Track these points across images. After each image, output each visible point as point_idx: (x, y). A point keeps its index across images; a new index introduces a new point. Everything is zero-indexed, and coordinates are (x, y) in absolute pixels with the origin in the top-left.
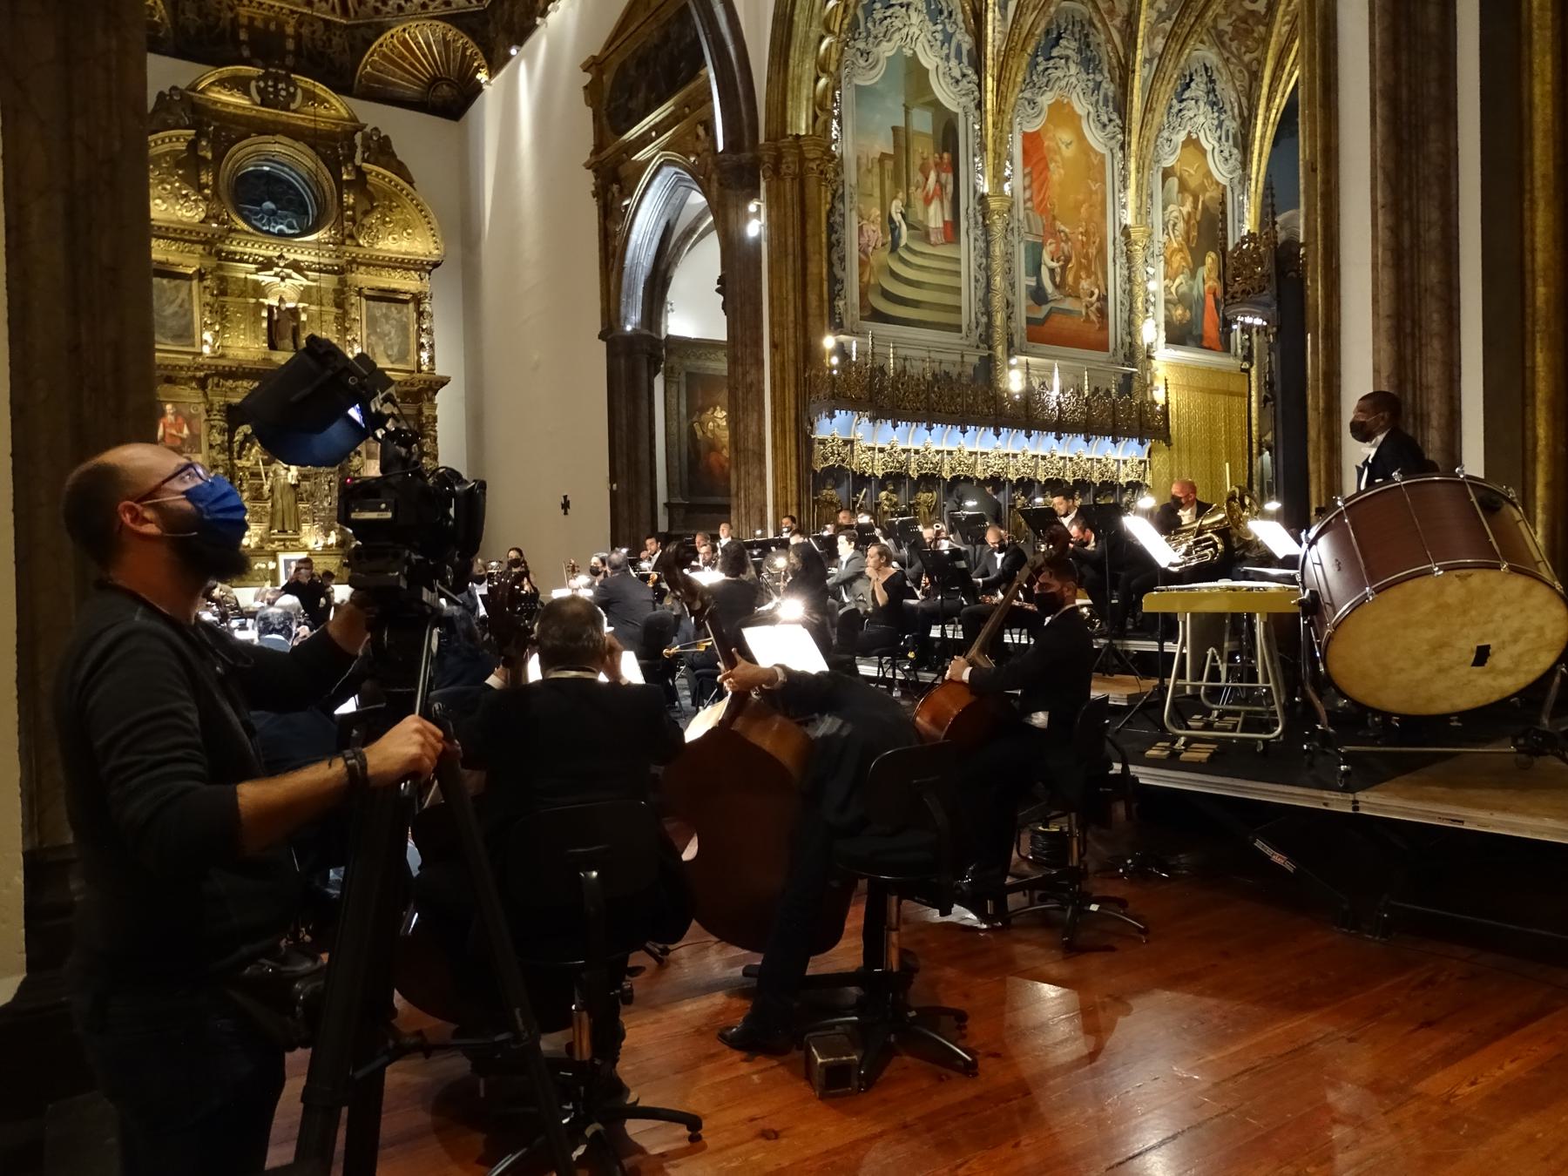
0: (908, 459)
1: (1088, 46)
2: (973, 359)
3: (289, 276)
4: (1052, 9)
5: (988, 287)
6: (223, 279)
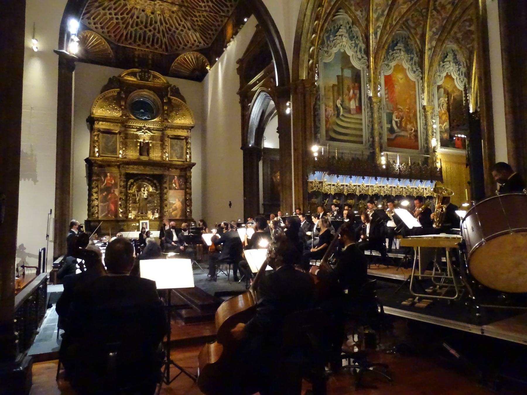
0: (343, 188)
1: (408, 45)
2: (367, 153)
3: (147, 132)
4: (394, 34)
5: (373, 129)
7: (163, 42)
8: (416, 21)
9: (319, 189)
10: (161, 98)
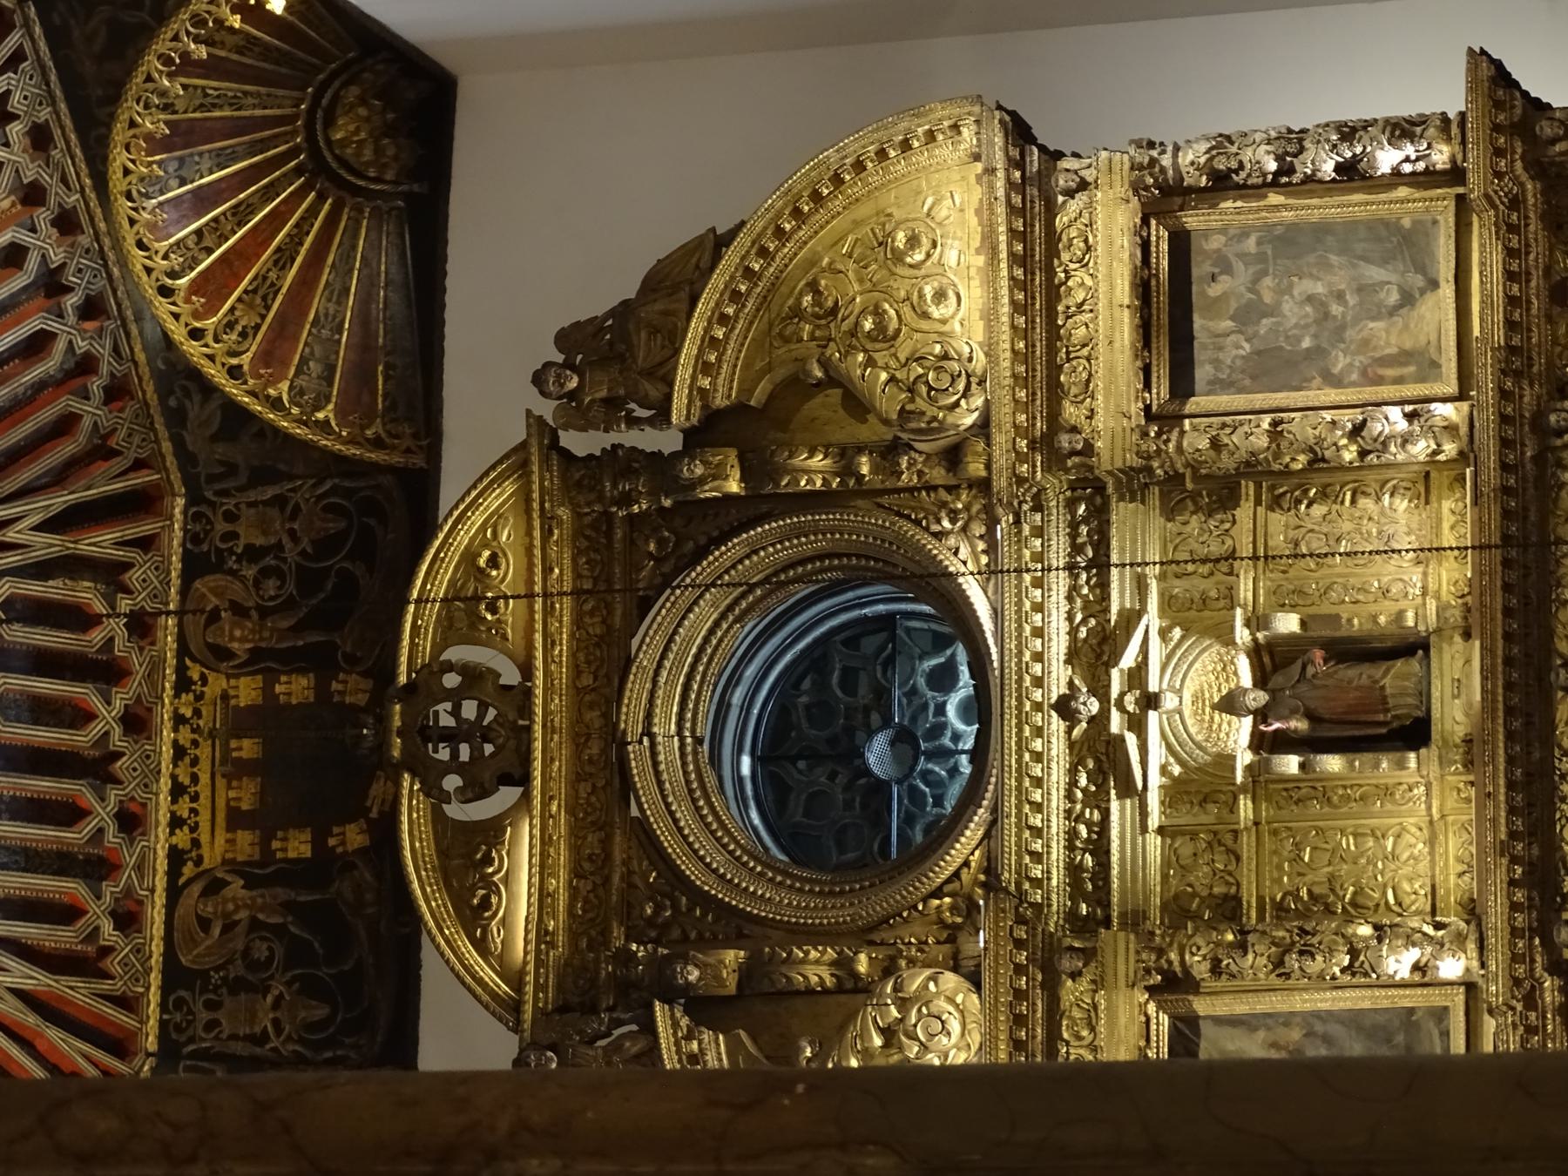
3: (1137, 676)
6: (1179, 912)
7: (49, 545)
10: (703, 526)
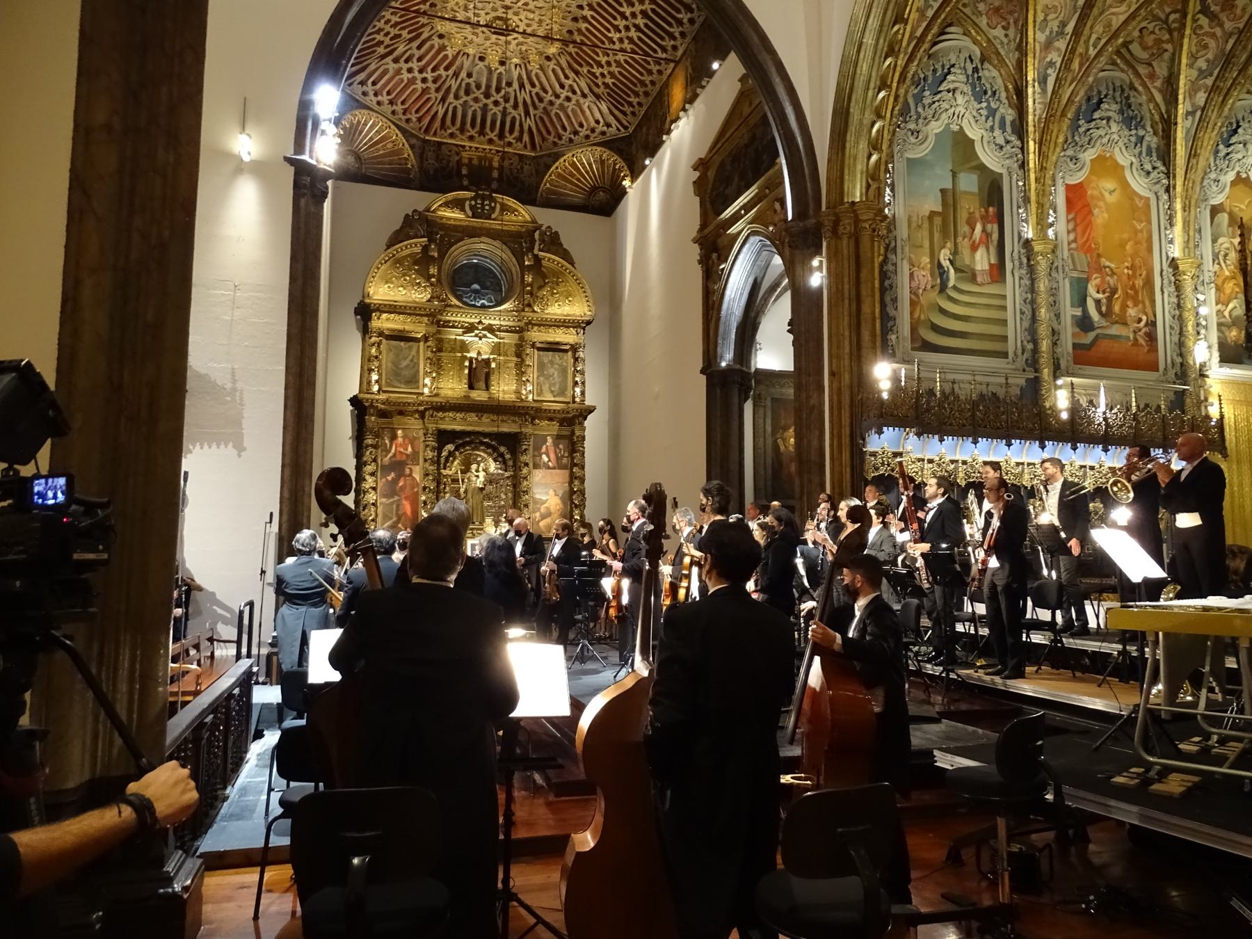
0: (956, 469)
1: (1129, 106)
2: (1019, 381)
3: (485, 336)
4: (1091, 79)
5: (1034, 319)
6: (440, 341)
7: (526, 128)
8: (1150, 44)
9: (893, 470)
